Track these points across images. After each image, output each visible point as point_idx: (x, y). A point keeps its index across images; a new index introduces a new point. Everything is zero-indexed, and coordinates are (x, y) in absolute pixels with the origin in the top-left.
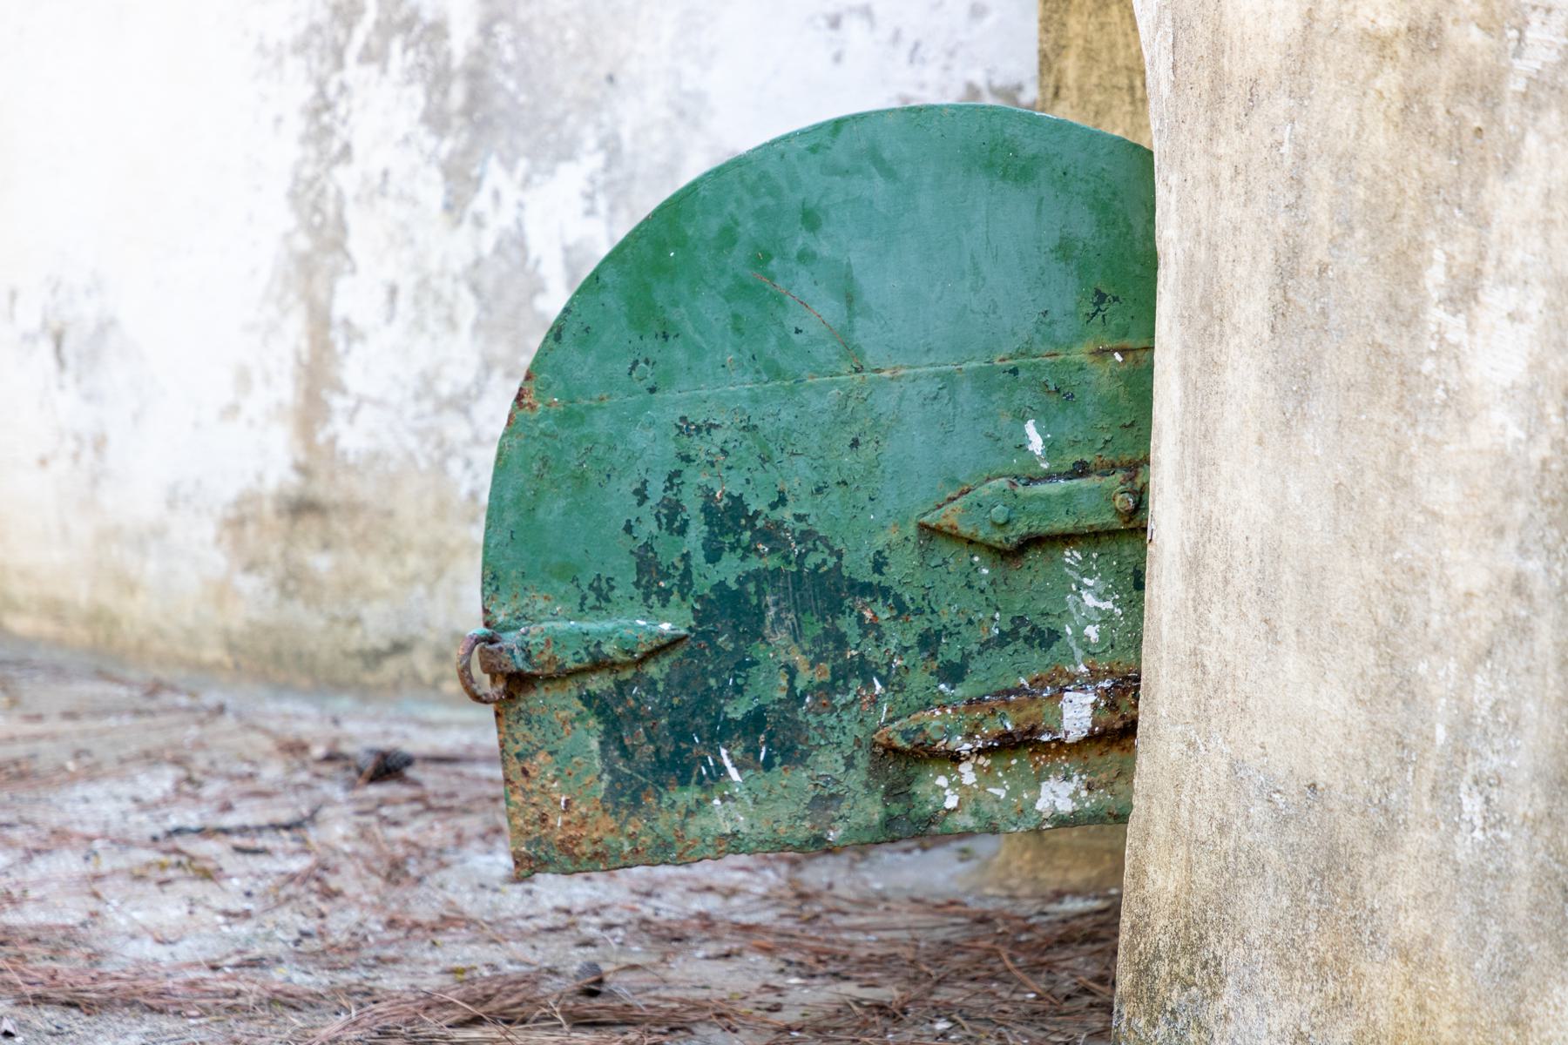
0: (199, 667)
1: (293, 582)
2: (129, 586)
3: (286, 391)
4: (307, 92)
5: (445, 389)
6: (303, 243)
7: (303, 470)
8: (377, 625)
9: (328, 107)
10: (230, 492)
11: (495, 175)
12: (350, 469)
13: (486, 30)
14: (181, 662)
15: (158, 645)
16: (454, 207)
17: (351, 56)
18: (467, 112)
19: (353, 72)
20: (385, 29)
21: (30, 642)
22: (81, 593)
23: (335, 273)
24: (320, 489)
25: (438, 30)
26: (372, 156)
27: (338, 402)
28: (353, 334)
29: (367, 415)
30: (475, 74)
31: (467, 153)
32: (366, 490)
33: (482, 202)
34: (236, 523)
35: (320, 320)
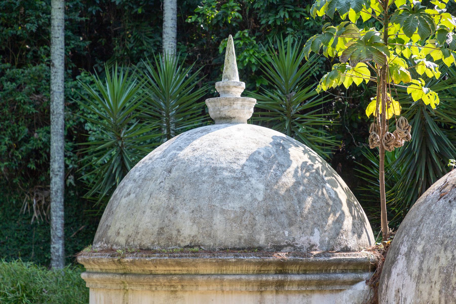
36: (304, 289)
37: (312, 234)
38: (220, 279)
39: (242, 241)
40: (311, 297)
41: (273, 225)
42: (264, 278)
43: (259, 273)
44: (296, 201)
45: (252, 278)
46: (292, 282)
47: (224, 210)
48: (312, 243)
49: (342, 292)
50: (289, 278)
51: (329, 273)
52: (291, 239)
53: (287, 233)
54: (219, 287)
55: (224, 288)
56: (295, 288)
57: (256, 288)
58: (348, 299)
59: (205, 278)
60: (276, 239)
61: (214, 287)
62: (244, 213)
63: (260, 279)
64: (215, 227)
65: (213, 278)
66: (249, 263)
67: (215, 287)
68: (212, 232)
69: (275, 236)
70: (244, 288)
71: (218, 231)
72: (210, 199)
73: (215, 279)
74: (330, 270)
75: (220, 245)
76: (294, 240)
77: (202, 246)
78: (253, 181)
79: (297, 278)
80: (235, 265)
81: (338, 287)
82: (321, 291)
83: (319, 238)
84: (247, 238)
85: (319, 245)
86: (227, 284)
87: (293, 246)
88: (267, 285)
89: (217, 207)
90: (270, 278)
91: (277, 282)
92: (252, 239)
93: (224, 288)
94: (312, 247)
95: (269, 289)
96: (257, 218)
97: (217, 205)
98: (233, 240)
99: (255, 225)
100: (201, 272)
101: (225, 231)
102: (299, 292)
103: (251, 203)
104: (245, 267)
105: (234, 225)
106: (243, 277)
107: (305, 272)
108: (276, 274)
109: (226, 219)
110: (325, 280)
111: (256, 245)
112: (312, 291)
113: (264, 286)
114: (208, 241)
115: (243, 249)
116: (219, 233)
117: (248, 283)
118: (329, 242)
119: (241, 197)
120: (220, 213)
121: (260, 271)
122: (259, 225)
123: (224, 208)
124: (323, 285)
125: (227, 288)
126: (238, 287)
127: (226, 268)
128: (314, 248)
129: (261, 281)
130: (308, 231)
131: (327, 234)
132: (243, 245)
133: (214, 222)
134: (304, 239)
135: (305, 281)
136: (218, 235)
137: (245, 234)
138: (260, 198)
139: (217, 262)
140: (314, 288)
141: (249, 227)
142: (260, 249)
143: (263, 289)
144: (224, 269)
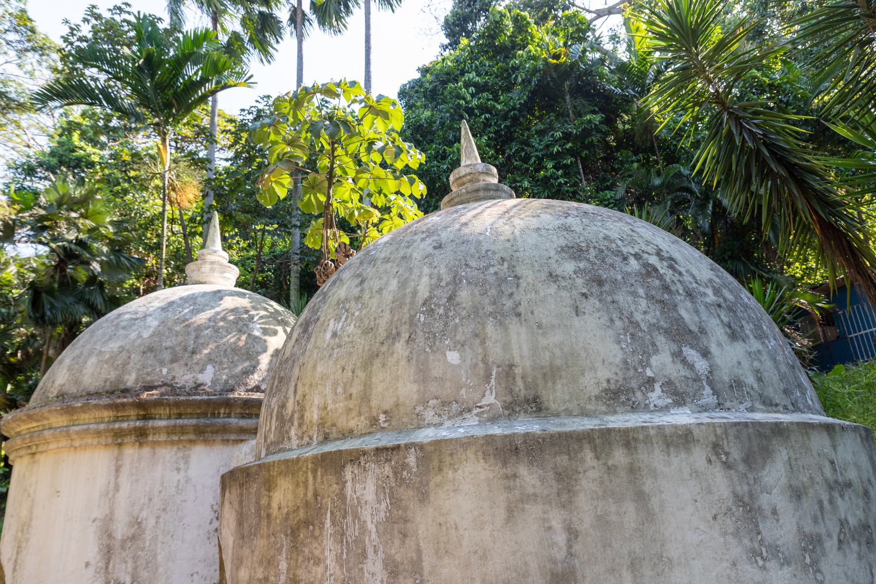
36: (175, 438)
37: (202, 371)
39: (108, 383)
40: (190, 449)
41: (150, 362)
42: (117, 426)
43: (117, 419)
44: (193, 336)
45: (102, 427)
46: (156, 430)
47: (101, 351)
48: (199, 382)
49: (243, 444)
50: (151, 423)
51: (219, 417)
52: (170, 378)
53: (165, 371)
56: (163, 437)
57: (110, 440)
58: (248, 451)
60: (149, 378)
61: (64, 443)
62: (121, 352)
63: (111, 427)
66: (96, 406)
69: (148, 374)
70: (95, 441)
73: (61, 432)
74: (219, 414)
75: (83, 391)
76: (174, 378)
78: (149, 319)
79: (162, 423)
80: (84, 412)
81: (233, 437)
82: (206, 442)
83: (212, 375)
84: (113, 379)
85: (210, 384)
86: (75, 437)
87: (171, 386)
88: (124, 435)
90: (125, 425)
91: (135, 429)
92: (119, 379)
94: (198, 386)
95: (127, 440)
96: (133, 356)
98: (97, 384)
99: (128, 364)
100: (54, 425)
101: (93, 374)
102: (173, 443)
103: (134, 341)
104: (98, 414)
105: (105, 366)
106: (91, 426)
107: (180, 416)
108: (138, 419)
109: (99, 361)
110: (207, 426)
111: (122, 387)
112: (191, 441)
113: (120, 436)
117: (98, 433)
118: (226, 382)
119: (126, 336)
121: (118, 417)
122: (132, 364)
124: (207, 432)
125: (77, 443)
128: (202, 387)
129: (113, 430)
130: (197, 368)
131: (226, 371)
132: (108, 388)
134: (186, 377)
135: (175, 426)
137: (113, 376)
138: (146, 335)
139: (62, 409)
140: (192, 437)
141: (120, 366)
142: (125, 391)
143: (119, 441)
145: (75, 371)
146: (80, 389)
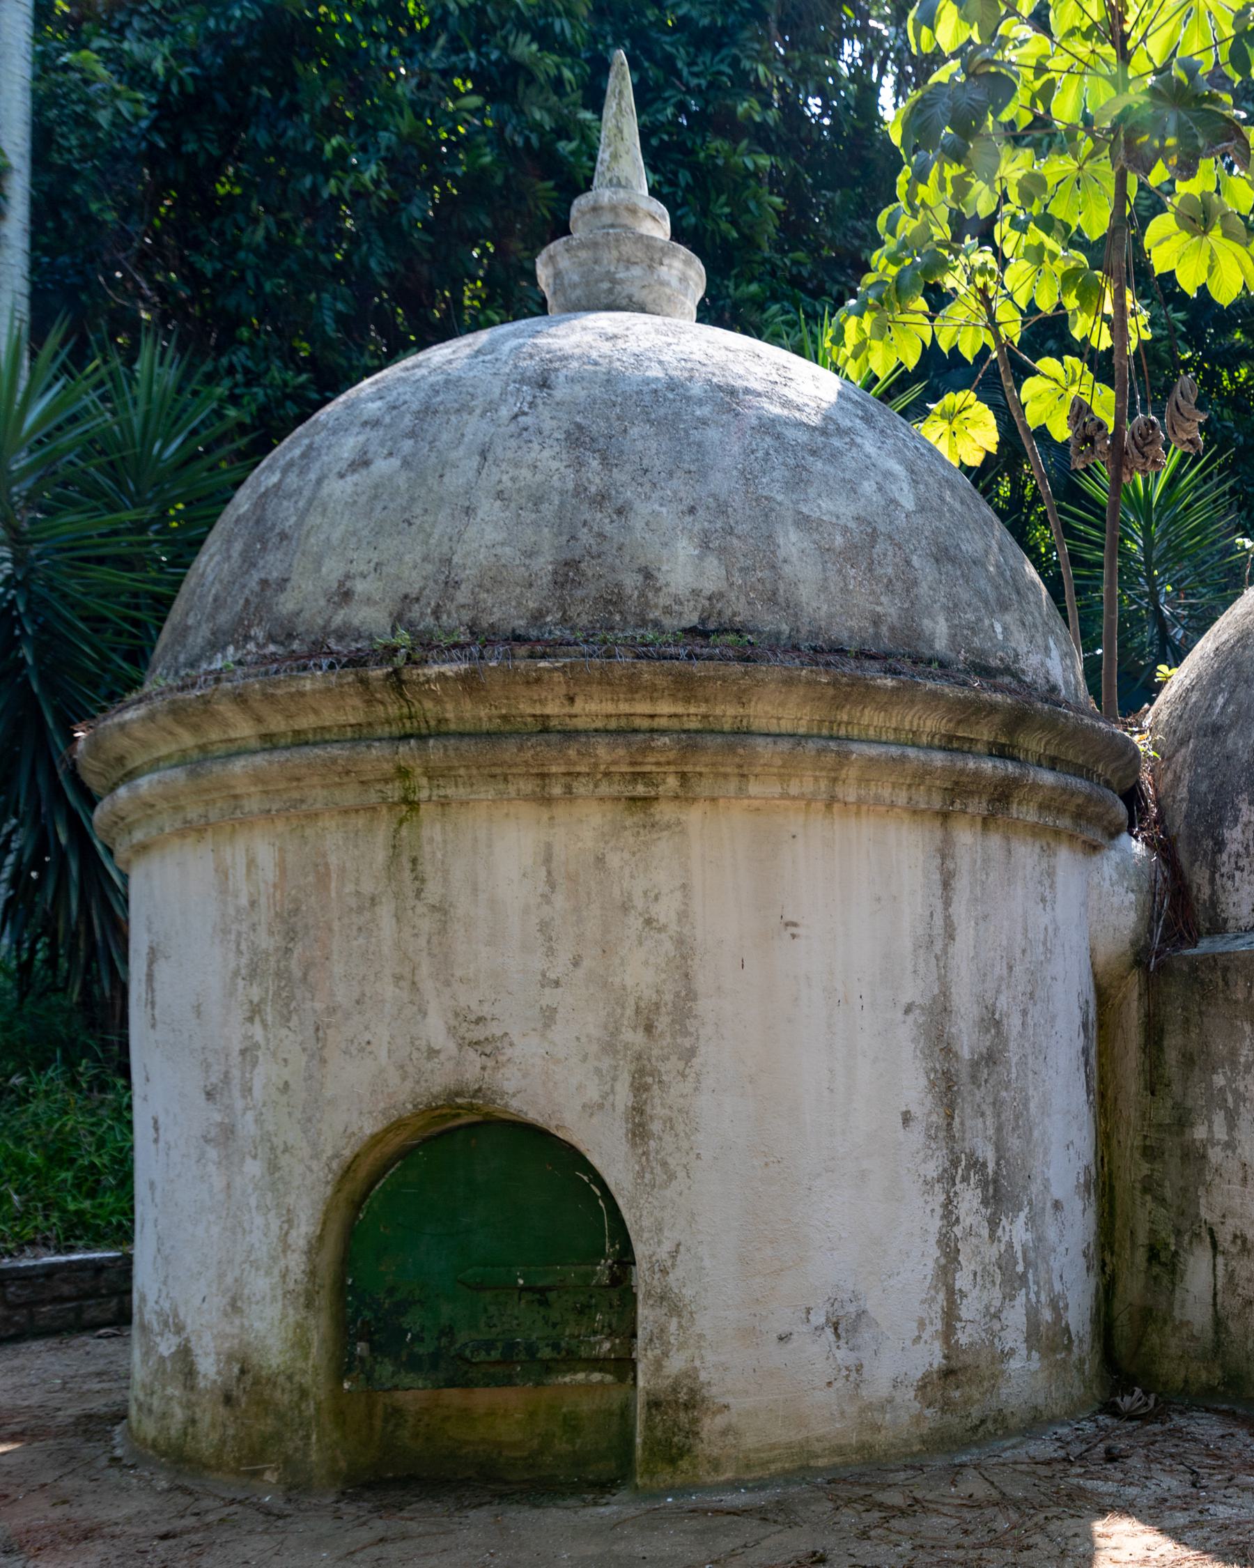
0: (913, 1455)
1: (947, 1406)
2: (878, 1429)
3: (939, 1325)
4: (942, 1197)
5: (992, 1310)
6: (943, 1261)
7: (946, 1357)
8: (976, 1412)
9: (951, 1202)
10: (919, 1375)
11: (1004, 1222)
12: (964, 1351)
13: (998, 1164)
14: (906, 1455)
15: (893, 1451)
16: (993, 1237)
17: (958, 1180)
18: (994, 1197)
19: (959, 1187)
20: (968, 1168)
21: (835, 1467)
22: (854, 1439)
23: (955, 1271)
24: (954, 1364)
25: (984, 1165)
26: (967, 1221)
27: (959, 1325)
28: (963, 1295)
29: (969, 1330)
30: (995, 1181)
31: (994, 1214)
32: (968, 1359)
33: (1000, 1232)
34: (923, 1387)
35: (951, 1292)
38: (838, 753)
54: (823, 784)
55: (840, 791)
59: (784, 745)
64: (787, 569)
65: (811, 745)
67: (808, 786)
68: (782, 587)
71: (801, 586)
72: (748, 477)
73: (820, 752)
75: (814, 634)
77: (751, 633)
89: (780, 504)
93: (840, 791)
97: (780, 498)
101: (824, 588)
114: (769, 618)
115: (886, 656)
116: (805, 593)
120: (797, 524)
123: (805, 510)
126: (886, 792)
127: (849, 714)
133: (781, 553)
136: (804, 599)
144: (845, 718)
145: (744, 562)
146: (804, 631)
